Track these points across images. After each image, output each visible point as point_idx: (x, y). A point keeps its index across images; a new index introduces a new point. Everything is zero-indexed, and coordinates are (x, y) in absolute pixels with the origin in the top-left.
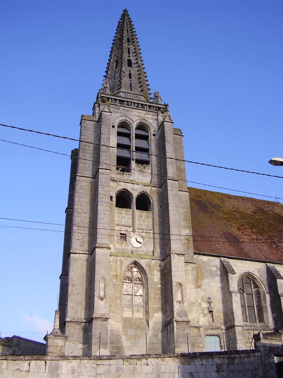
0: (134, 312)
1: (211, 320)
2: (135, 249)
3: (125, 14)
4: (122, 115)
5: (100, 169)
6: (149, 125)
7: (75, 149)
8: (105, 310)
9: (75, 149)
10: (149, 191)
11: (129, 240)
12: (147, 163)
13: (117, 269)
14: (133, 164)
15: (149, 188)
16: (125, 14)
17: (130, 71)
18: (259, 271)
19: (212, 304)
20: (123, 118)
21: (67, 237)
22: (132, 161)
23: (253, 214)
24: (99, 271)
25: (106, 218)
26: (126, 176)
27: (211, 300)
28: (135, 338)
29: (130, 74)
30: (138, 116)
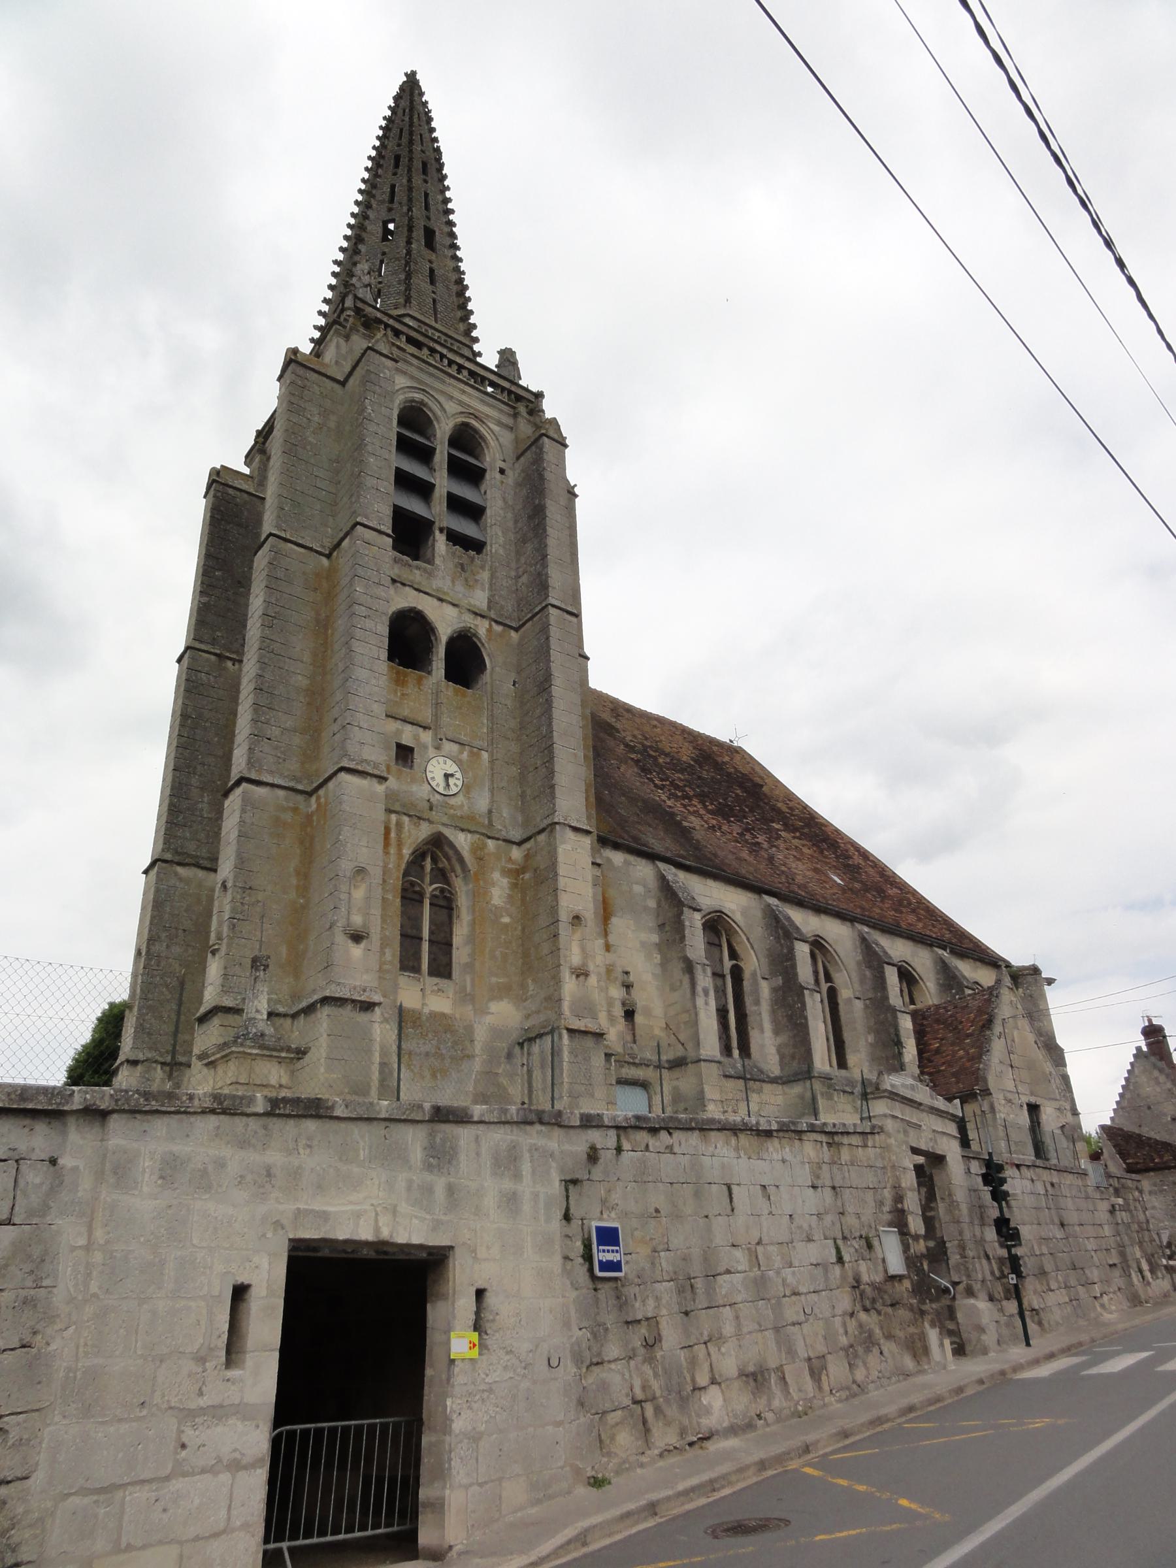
0: (428, 992)
1: (629, 1038)
2: (438, 796)
3: (410, 91)
4: (415, 385)
5: (362, 528)
6: (489, 438)
7: (222, 466)
8: (365, 977)
9: (222, 466)
10: (484, 630)
11: (423, 769)
12: (477, 546)
13: (168, 890)
14: (440, 543)
15: (486, 623)
16: (410, 91)
17: (430, 262)
18: (744, 913)
19: (633, 991)
20: (418, 396)
21: (185, 739)
22: (437, 533)
23: (692, 763)
24: (349, 845)
25: (374, 681)
26: (416, 576)
27: (632, 978)
28: (434, 1076)
29: (432, 271)
30: (461, 403)
